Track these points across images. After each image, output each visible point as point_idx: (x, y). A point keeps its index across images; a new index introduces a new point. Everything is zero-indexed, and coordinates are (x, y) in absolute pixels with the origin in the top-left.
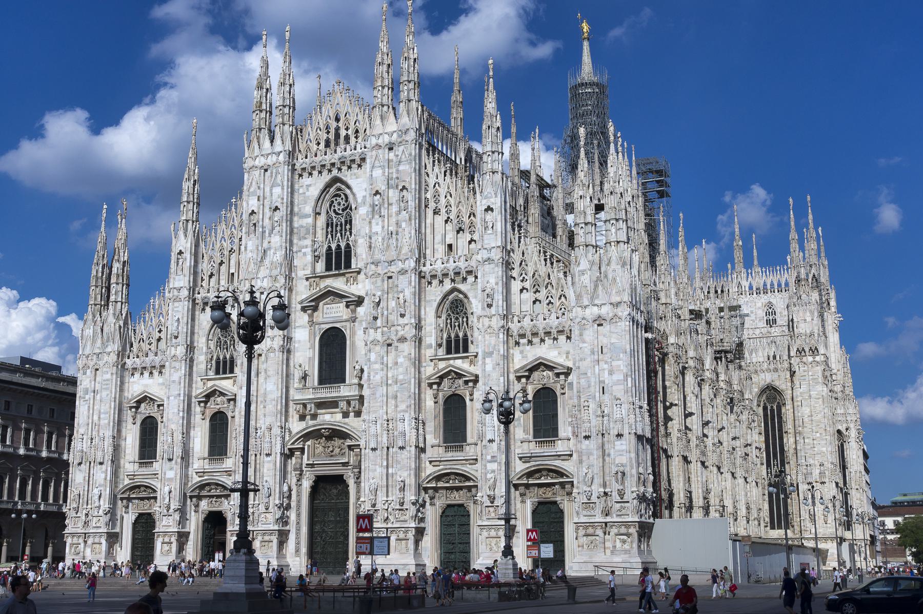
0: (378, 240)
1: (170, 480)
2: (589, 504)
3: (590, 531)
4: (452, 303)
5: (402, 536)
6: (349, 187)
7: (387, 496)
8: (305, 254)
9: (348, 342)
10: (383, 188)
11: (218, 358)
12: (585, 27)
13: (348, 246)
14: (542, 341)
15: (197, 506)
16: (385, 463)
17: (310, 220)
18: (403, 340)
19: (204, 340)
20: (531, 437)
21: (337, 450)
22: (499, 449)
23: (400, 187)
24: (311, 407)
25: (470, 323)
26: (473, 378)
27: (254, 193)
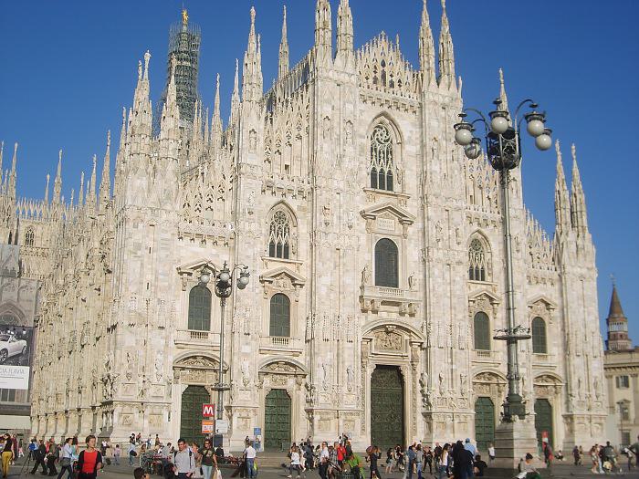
0: (437, 178)
1: (246, 355)
2: (581, 403)
3: (581, 420)
5: (462, 420)
6: (392, 121)
7: (452, 387)
9: (400, 254)
10: (440, 137)
12: (186, 18)
13: (390, 171)
16: (450, 361)
18: (459, 263)
24: (378, 304)
25: (487, 259)
27: (328, 102)
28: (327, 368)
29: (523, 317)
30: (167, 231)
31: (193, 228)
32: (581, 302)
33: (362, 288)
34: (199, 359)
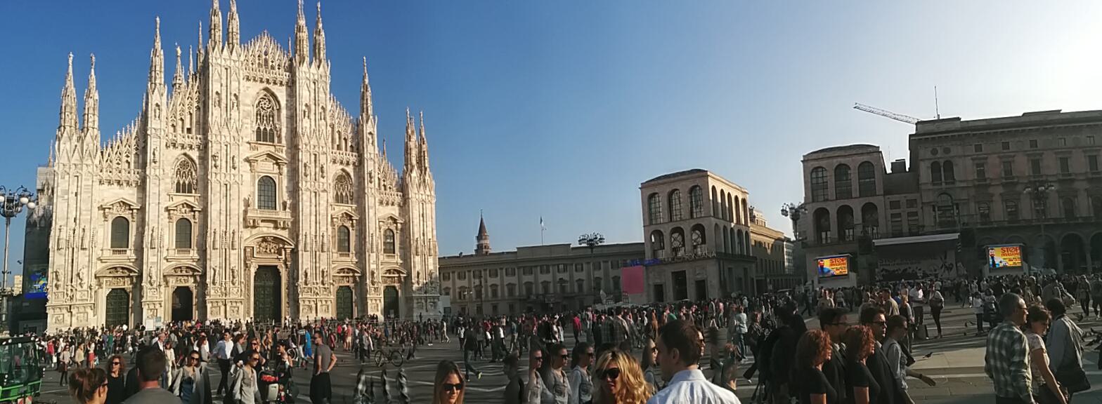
3: (420, 300)
4: (339, 176)
7: (316, 280)
8: (246, 127)
11: (178, 183)
13: (271, 130)
14: (387, 204)
15: (167, 283)
17: (250, 108)
18: (325, 191)
19: (169, 168)
20: (382, 252)
21: (272, 251)
22: (377, 257)
23: (320, 106)
26: (357, 218)
28: (217, 269)
29: (374, 229)
30: (88, 180)
31: (114, 176)
32: (421, 218)
33: (246, 212)
34: (118, 269)
